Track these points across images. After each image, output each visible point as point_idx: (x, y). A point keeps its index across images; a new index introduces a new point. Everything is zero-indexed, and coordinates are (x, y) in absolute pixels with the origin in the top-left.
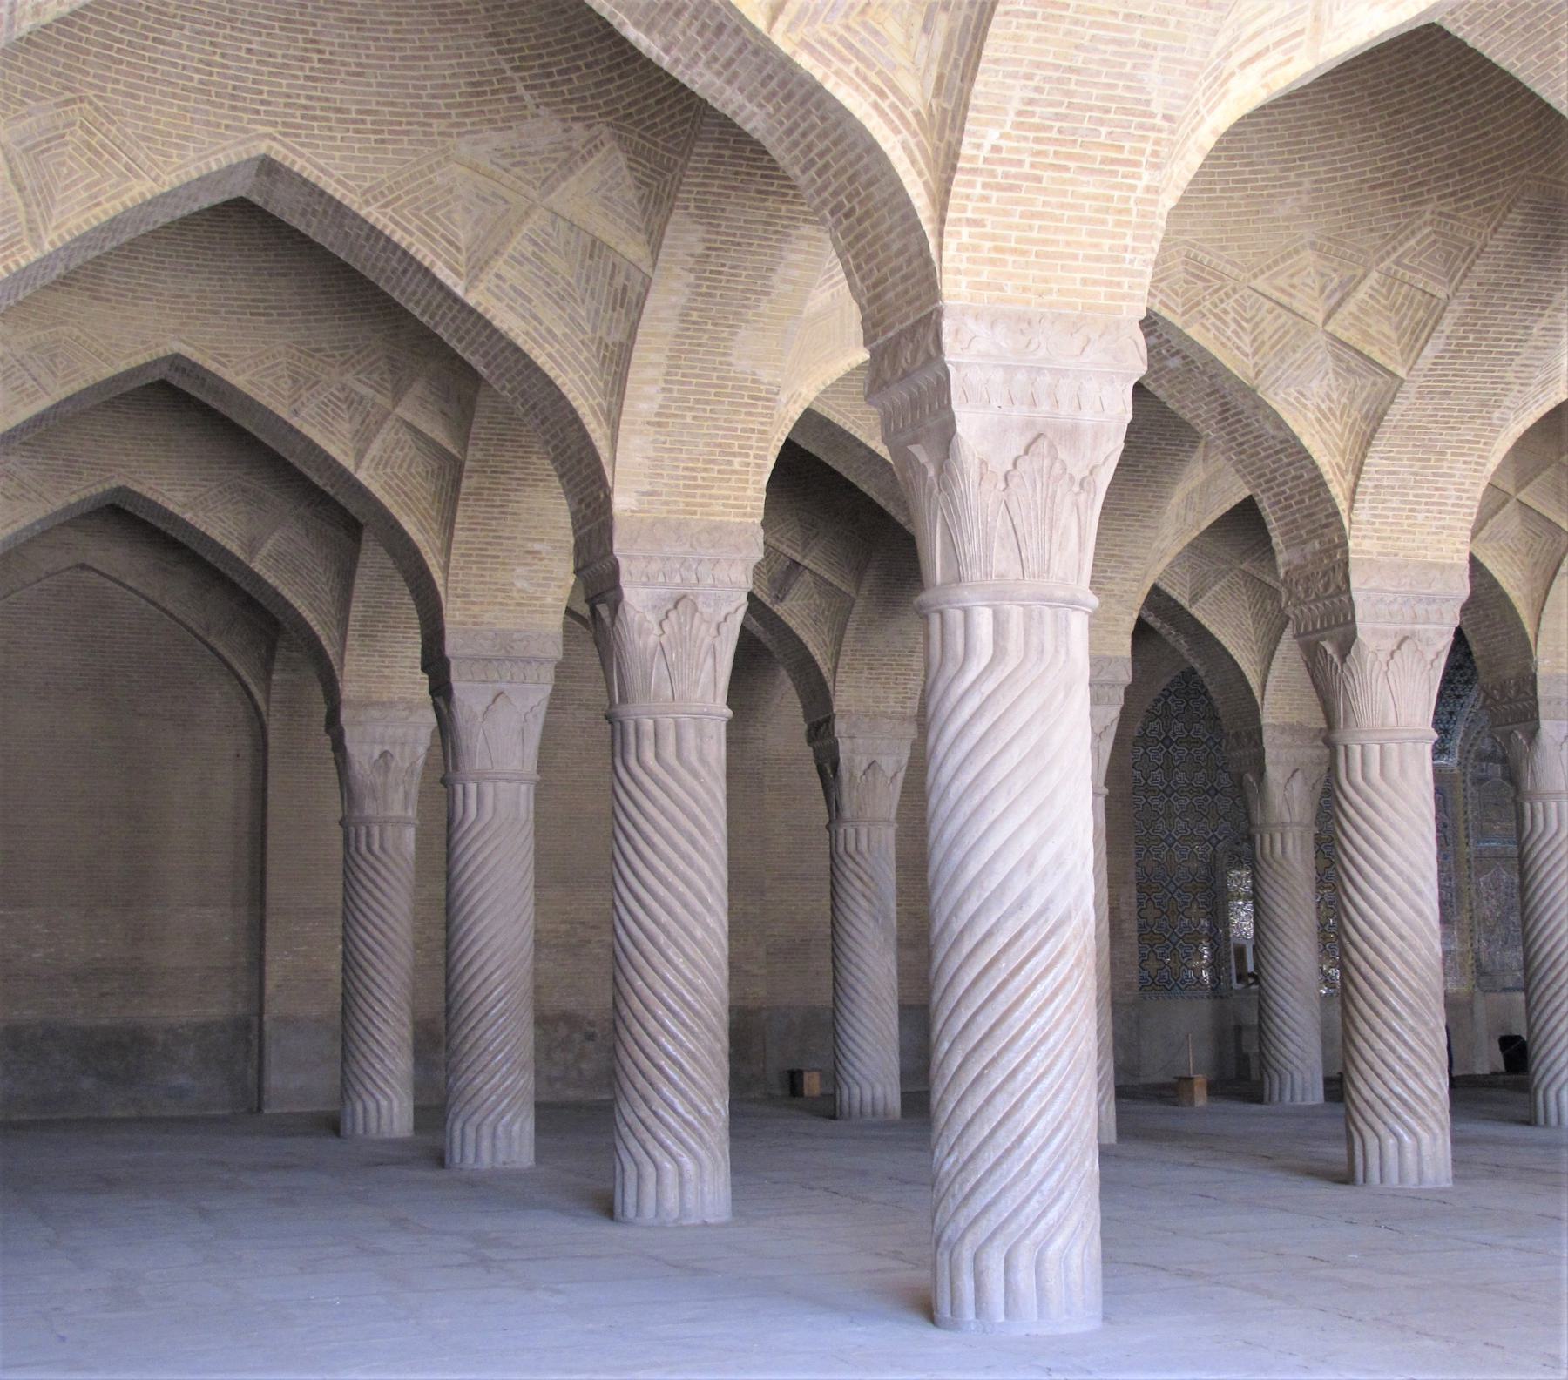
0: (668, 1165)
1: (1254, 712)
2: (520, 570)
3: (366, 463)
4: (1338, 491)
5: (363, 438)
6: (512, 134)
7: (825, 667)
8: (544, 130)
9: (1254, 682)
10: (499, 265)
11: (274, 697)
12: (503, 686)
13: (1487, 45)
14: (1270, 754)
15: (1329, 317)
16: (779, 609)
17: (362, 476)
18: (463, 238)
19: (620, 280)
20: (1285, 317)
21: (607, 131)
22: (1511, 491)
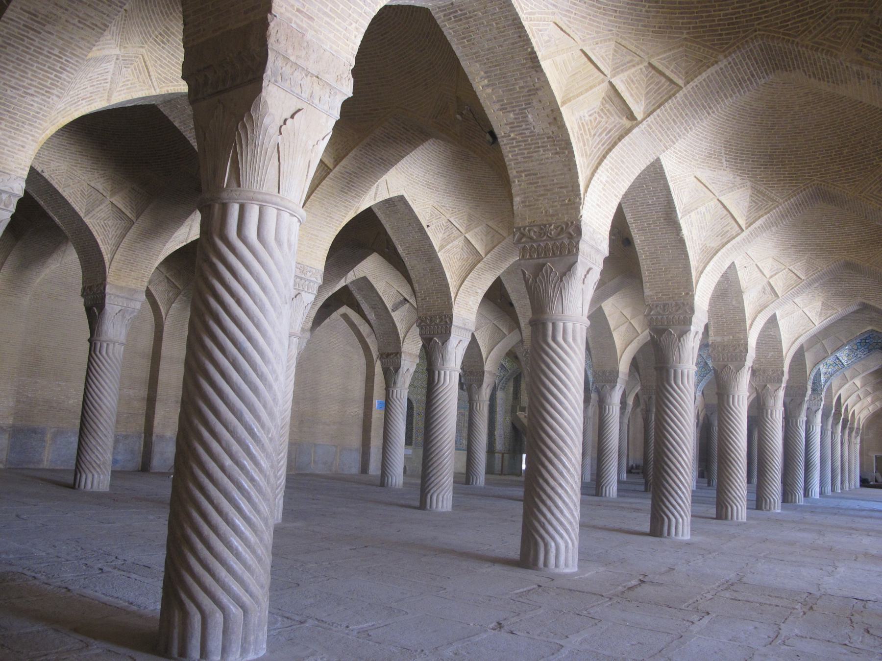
0: (674, 520)
1: (482, 366)
2: (472, 298)
3: (443, 250)
4: (748, 323)
5: (446, 242)
6: (715, 173)
7: (401, 336)
8: (726, 176)
9: (484, 357)
10: (693, 214)
11: (170, 312)
12: (461, 338)
13: (616, 196)
14: (485, 379)
15: (771, 277)
16: (393, 314)
17: (440, 255)
18: (684, 201)
19: (728, 228)
20: (760, 275)
21: (749, 184)
22: (629, 317)
